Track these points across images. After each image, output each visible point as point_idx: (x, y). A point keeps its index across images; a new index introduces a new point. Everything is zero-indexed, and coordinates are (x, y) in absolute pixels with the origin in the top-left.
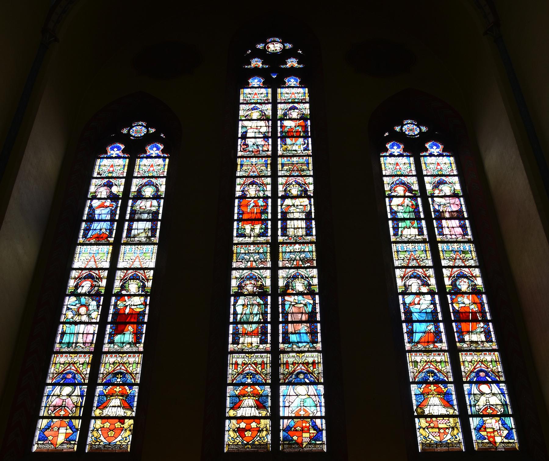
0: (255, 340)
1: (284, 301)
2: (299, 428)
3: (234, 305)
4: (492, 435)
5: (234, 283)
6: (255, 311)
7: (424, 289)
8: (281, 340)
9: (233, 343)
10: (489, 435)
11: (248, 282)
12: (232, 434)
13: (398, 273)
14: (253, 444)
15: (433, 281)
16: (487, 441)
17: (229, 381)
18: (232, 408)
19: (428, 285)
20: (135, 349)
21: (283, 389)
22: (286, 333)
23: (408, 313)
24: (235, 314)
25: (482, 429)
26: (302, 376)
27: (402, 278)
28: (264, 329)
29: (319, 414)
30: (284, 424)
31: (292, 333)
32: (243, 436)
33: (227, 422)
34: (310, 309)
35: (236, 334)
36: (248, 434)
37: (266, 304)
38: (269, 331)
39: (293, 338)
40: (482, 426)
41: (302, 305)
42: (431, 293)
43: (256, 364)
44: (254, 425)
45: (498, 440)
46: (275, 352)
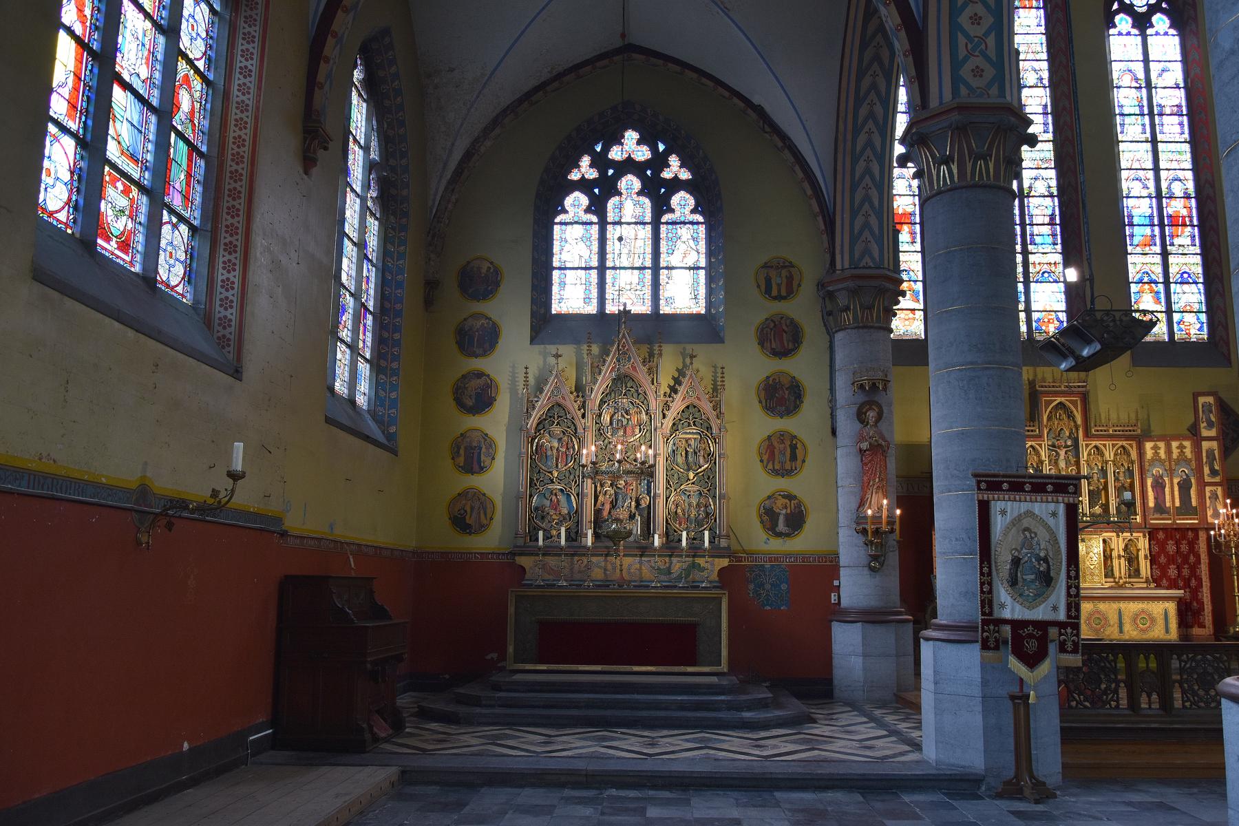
2: (1046, 320)
4: (1188, 327)
10: (1186, 327)
16: (1184, 332)
25: (1182, 323)
30: (1035, 316)
40: (1181, 320)
45: (1193, 331)
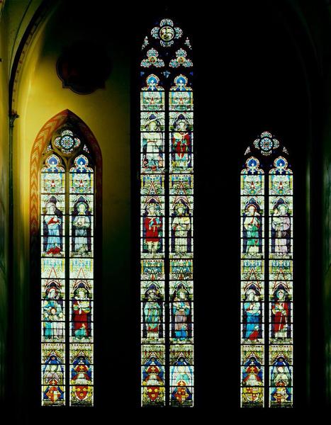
0: (156, 335)
1: (172, 306)
2: (180, 393)
3: (143, 309)
5: (143, 292)
6: (156, 314)
7: (257, 299)
8: (170, 336)
9: (144, 337)
11: (151, 291)
12: (145, 396)
13: (243, 284)
14: (156, 402)
15: (262, 292)
17: (142, 363)
18: (144, 380)
19: (259, 295)
20: (88, 341)
21: (171, 368)
22: (173, 330)
23: (245, 316)
24: (144, 316)
26: (182, 360)
27: (244, 288)
28: (161, 326)
29: (190, 385)
31: (177, 330)
32: (150, 397)
33: (142, 388)
34: (187, 313)
35: (145, 331)
36: (153, 396)
37: (162, 309)
38: (164, 329)
39: (178, 334)
41: (183, 310)
42: (260, 301)
43: (157, 352)
44: (156, 390)
46: (168, 344)
